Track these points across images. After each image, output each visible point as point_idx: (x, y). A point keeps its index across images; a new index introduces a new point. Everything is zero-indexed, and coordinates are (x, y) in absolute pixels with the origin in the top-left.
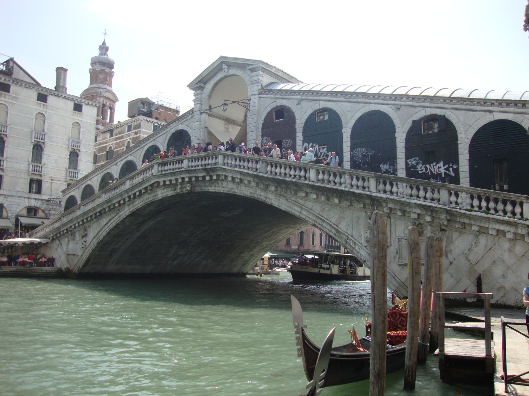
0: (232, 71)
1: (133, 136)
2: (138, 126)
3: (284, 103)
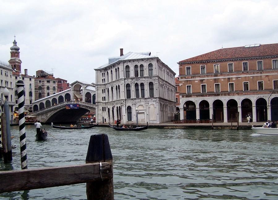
0: (79, 84)
1: (42, 84)
2: (44, 82)
3: (89, 92)
